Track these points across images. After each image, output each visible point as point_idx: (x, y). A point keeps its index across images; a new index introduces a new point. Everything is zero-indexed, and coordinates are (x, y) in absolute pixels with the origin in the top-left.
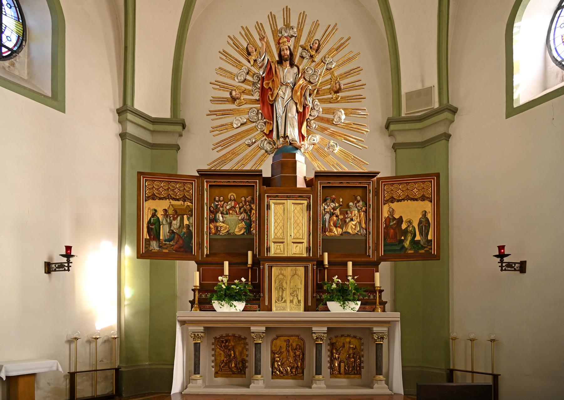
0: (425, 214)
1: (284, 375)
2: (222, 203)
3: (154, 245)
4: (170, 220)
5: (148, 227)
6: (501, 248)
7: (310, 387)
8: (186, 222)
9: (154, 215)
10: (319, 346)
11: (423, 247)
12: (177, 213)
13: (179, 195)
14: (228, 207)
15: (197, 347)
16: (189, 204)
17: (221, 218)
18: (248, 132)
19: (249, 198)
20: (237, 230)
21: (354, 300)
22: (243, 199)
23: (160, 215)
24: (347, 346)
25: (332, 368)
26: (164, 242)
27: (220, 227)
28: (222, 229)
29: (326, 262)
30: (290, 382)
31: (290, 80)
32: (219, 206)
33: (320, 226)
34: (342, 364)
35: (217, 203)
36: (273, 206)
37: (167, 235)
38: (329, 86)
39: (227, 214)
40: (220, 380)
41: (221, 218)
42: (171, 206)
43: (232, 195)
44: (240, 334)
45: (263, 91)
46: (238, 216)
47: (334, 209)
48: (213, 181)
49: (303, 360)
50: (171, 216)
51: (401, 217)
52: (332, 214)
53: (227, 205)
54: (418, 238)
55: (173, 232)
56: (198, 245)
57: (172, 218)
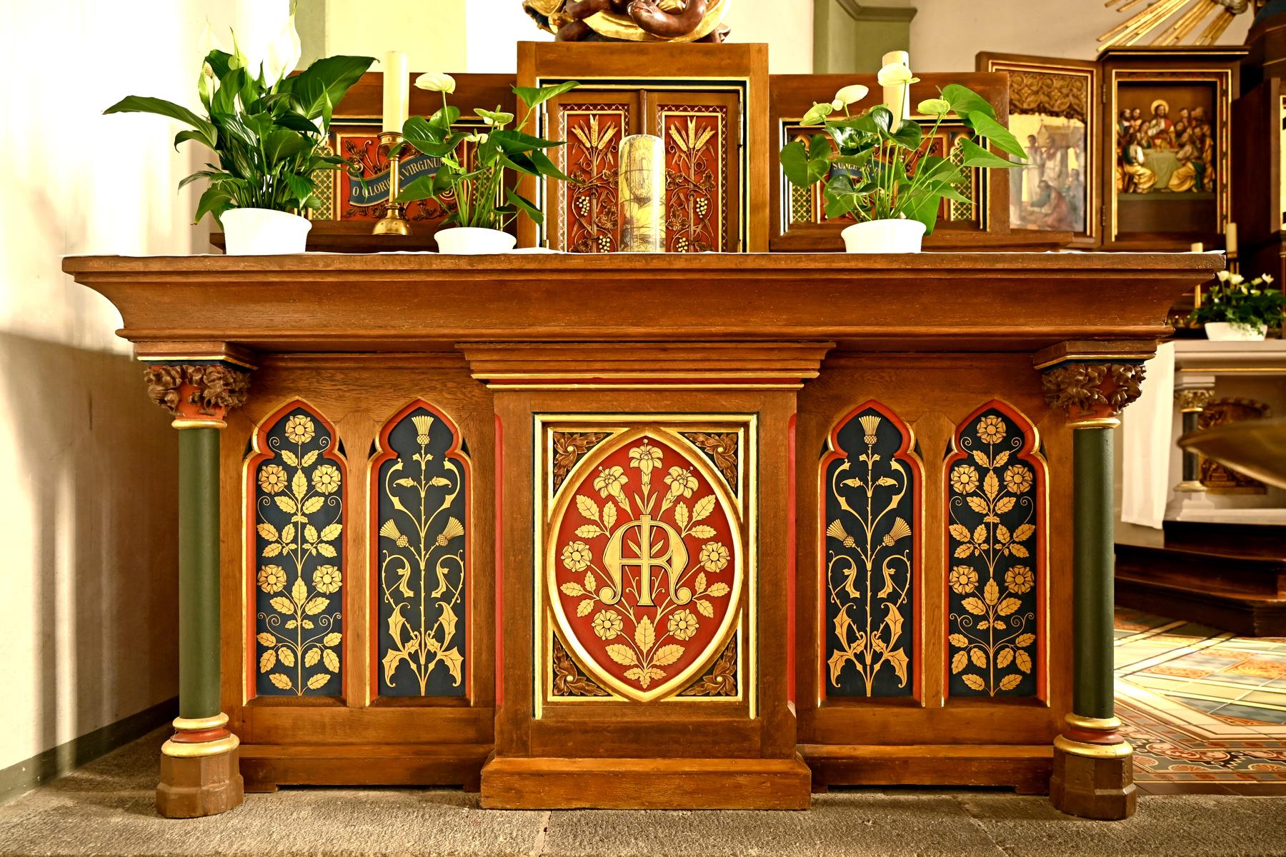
2: (1139, 122)
4: (1041, 158)
14: (1152, 132)
16: (1080, 124)
17: (1141, 158)
19: (1198, 112)
20: (1174, 182)
22: (1185, 113)
26: (1029, 208)
27: (1139, 175)
28: (1142, 181)
32: (1131, 131)
35: (1126, 124)
37: (1036, 193)
39: (1149, 147)
41: (1141, 158)
42: (1043, 130)
43: (1160, 103)
44: (1254, 397)
46: (1176, 150)
50: (1043, 150)
53: (1149, 128)
55: (1048, 187)
56: (1099, 216)
57: (1045, 156)
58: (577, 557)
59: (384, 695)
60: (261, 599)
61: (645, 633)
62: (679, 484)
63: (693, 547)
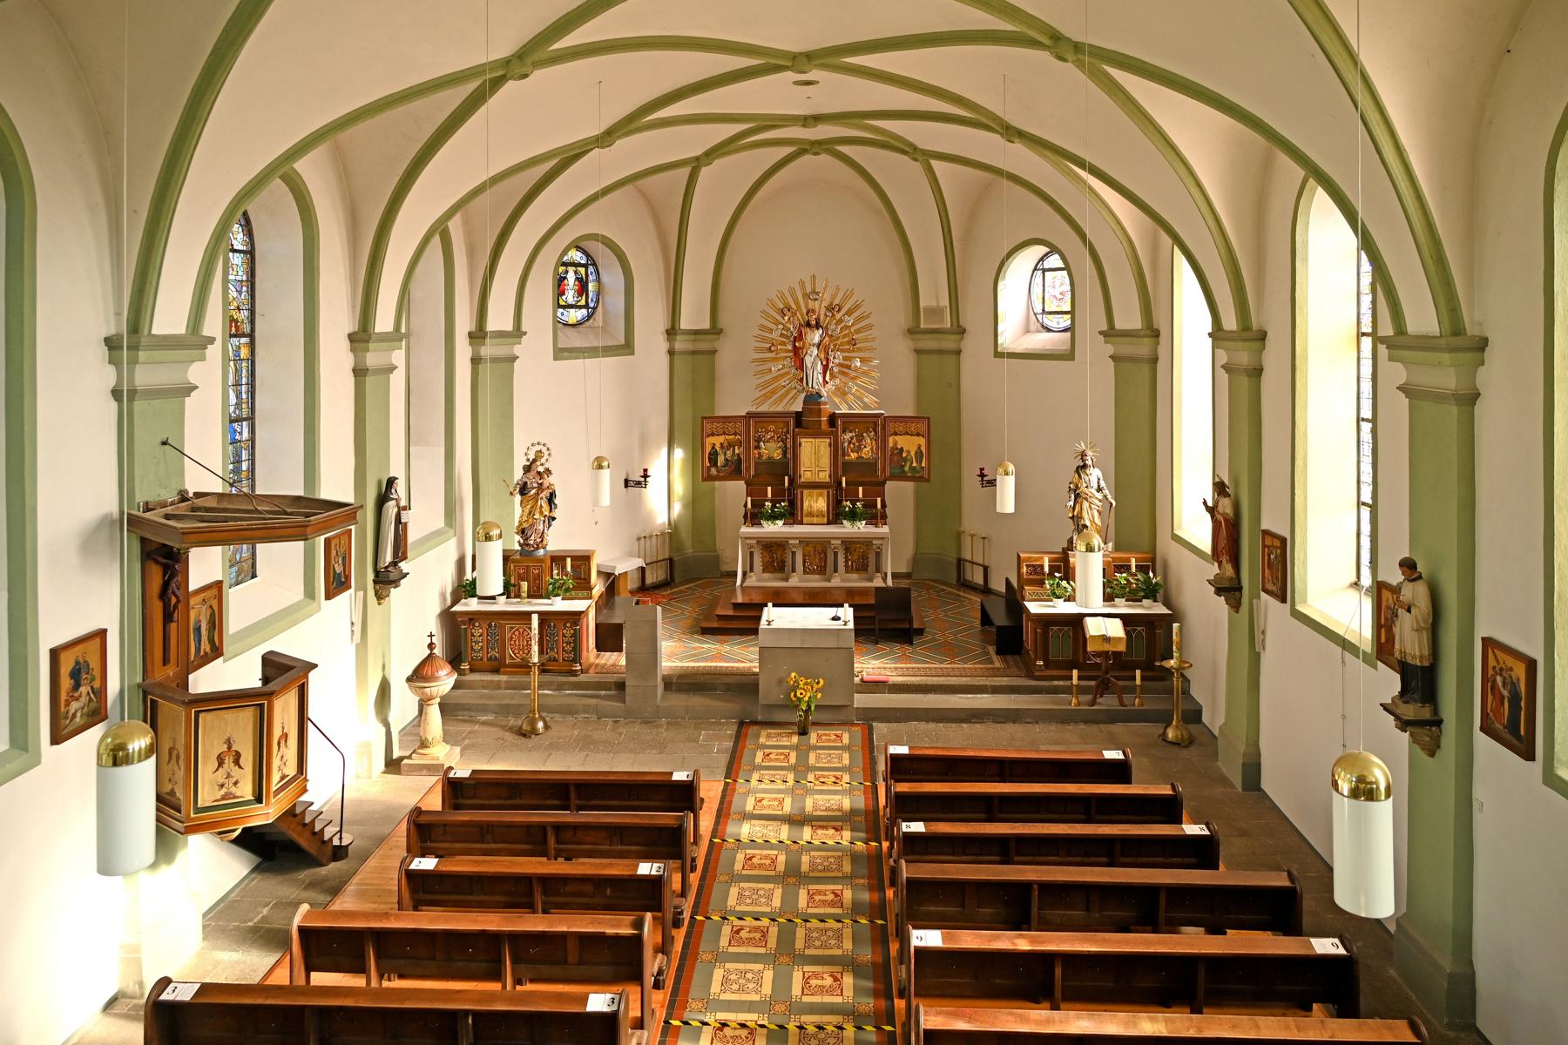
0: (919, 447)
1: (812, 572)
3: (713, 471)
5: (709, 458)
6: (982, 469)
7: (830, 581)
8: (737, 451)
9: (713, 448)
10: (836, 554)
11: (918, 472)
12: (731, 445)
13: (732, 431)
15: (752, 554)
18: (782, 376)
19: (785, 430)
21: (860, 520)
23: (717, 448)
24: (857, 550)
25: (846, 566)
29: (844, 485)
30: (817, 577)
31: (817, 339)
33: (840, 452)
34: (854, 564)
36: (803, 444)
38: (847, 339)
40: (766, 575)
43: (772, 427)
45: (796, 350)
47: (852, 438)
48: (757, 419)
49: (825, 561)
51: (902, 448)
52: (850, 443)
54: (914, 464)
55: (727, 460)
58: (512, 642)
59: (488, 660)
60: (472, 647)
61: (521, 652)
62: (525, 633)
63: (527, 641)
